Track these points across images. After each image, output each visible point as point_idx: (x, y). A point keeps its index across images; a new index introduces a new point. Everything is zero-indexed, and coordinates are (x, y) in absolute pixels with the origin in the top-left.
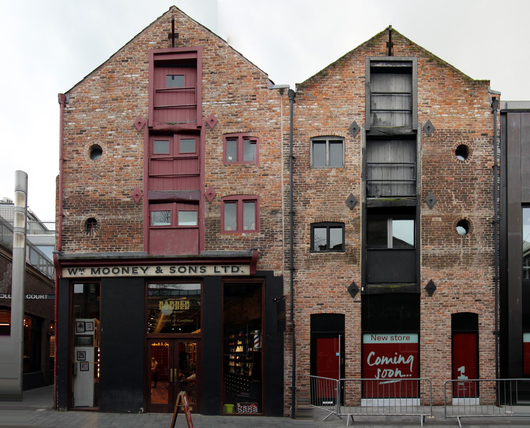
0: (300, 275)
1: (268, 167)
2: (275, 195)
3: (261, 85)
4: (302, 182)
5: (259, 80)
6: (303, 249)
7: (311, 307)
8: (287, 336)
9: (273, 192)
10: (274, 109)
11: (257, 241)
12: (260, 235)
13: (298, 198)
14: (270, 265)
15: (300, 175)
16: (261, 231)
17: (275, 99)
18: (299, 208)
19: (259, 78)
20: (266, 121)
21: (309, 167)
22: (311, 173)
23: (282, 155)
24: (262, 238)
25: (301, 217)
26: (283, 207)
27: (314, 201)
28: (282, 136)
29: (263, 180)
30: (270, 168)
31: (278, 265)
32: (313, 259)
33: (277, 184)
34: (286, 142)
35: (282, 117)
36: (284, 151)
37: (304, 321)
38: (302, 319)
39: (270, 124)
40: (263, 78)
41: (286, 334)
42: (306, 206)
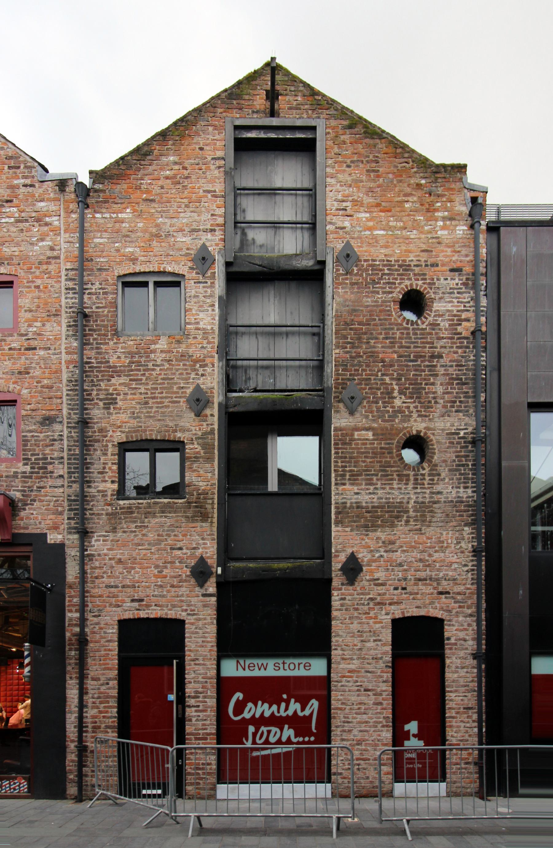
0: (98, 544)
1: (35, 333)
2: (50, 387)
3: (22, 181)
4: (101, 363)
5: (18, 171)
6: (103, 493)
7: (119, 606)
8: (73, 653)
9: (45, 382)
10: (47, 219)
11: (17, 477)
12: (21, 468)
13: (95, 393)
14: (40, 523)
15: (97, 348)
16: (24, 459)
17: (49, 200)
18: (96, 413)
19: (19, 167)
20: (32, 244)
21: (116, 334)
22: (120, 346)
23: (63, 310)
24: (25, 472)
25: (101, 430)
26: (65, 412)
27: (126, 399)
28: (63, 273)
29: (27, 359)
30: (39, 334)
31: (54, 523)
32: (123, 513)
33: (53, 367)
34: (71, 284)
35: (64, 236)
36: (67, 301)
37: (105, 633)
38: (101, 628)
39: (39, 249)
40: (26, 167)
41: (70, 650)
42: (109, 408)
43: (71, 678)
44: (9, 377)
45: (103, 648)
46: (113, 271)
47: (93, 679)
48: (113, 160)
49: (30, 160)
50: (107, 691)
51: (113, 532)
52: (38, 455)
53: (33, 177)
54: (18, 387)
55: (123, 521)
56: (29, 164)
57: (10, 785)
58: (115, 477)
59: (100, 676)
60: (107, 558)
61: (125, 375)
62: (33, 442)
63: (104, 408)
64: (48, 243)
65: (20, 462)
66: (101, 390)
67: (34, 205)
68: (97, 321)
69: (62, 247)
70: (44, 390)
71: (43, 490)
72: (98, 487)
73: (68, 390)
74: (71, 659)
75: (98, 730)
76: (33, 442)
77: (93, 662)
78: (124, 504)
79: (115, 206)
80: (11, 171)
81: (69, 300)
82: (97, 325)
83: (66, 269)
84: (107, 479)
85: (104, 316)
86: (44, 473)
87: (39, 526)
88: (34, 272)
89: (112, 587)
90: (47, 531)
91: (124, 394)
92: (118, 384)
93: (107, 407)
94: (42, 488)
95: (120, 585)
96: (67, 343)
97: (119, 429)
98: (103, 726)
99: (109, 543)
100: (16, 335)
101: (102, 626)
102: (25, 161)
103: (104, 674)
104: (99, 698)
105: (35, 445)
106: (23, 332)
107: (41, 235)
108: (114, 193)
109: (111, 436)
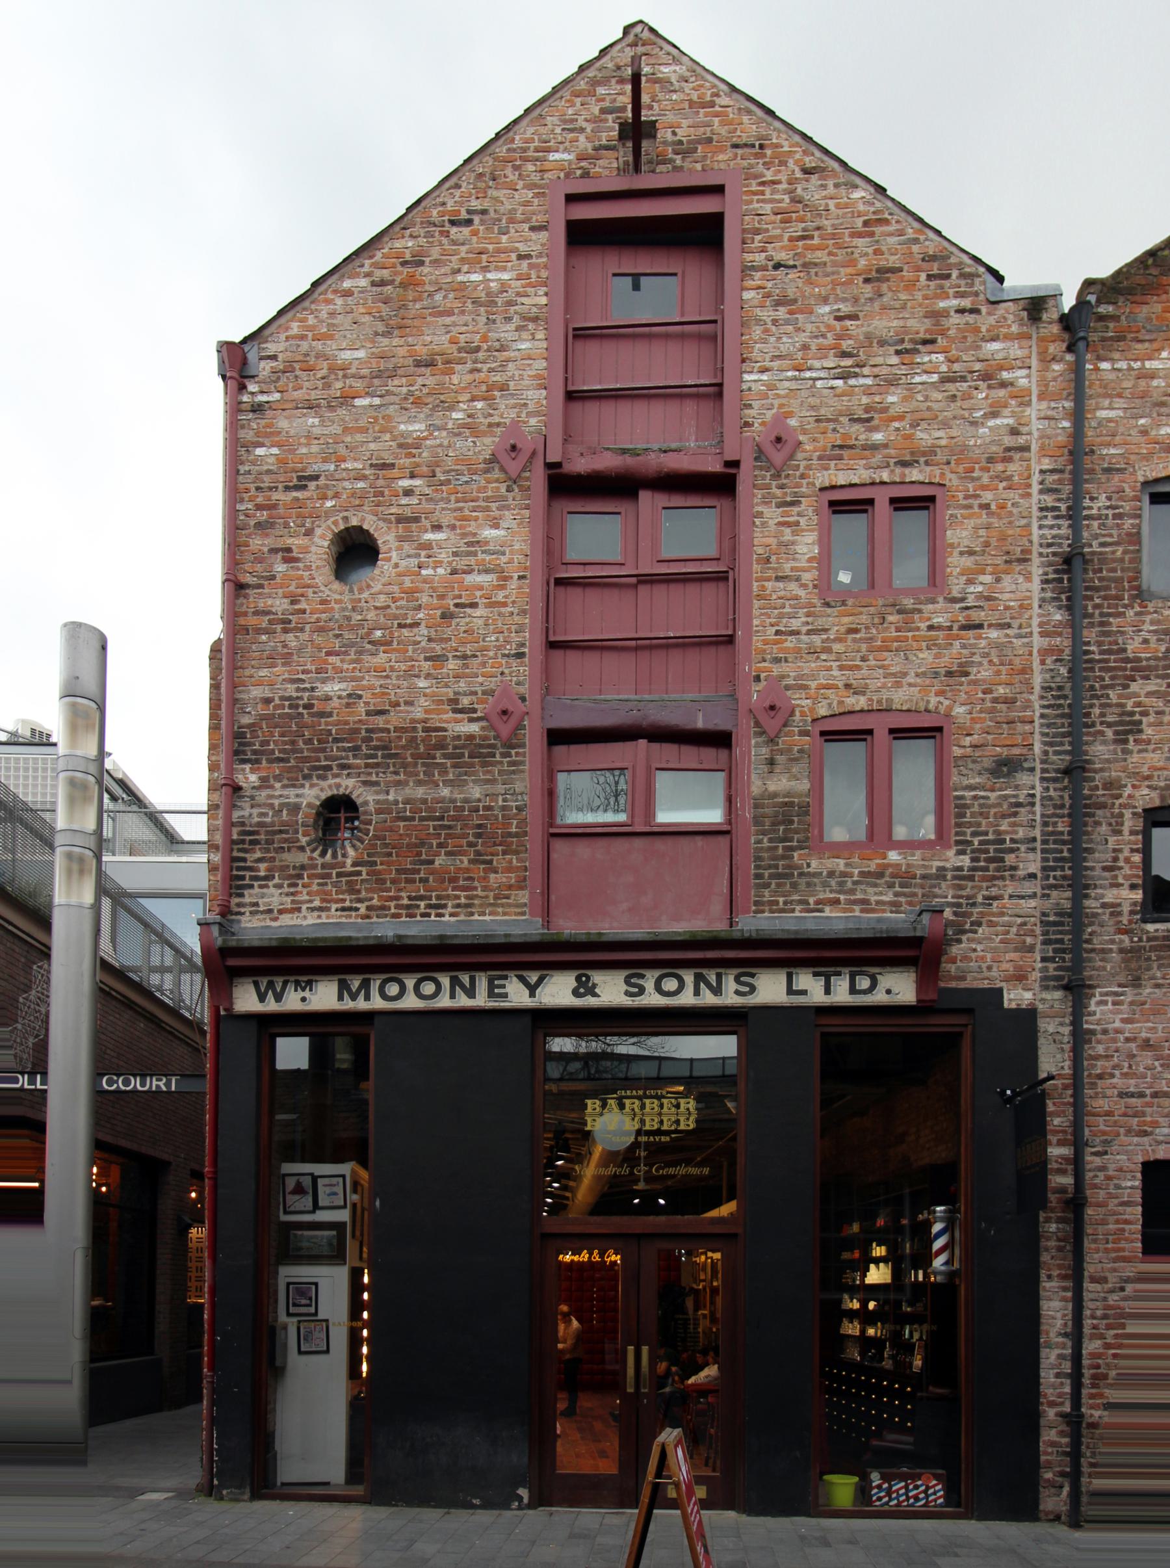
0: (1102, 1011)
1: (980, 596)
2: (1009, 701)
3: (955, 302)
4: (1110, 652)
5: (947, 283)
6: (1114, 909)
7: (1145, 1134)
8: (1053, 1227)
9: (1001, 690)
10: (1005, 375)
11: (944, 878)
12: (953, 859)
13: (1097, 711)
14: (989, 968)
15: (1102, 624)
16: (958, 843)
17: (1008, 337)
18: (1100, 751)
19: (948, 276)
20: (974, 423)
21: (1141, 595)
22: (1148, 618)
23: (1036, 549)
24: (960, 869)
25: (1109, 785)
26: (1038, 748)
27: (1161, 724)
28: (1036, 478)
29: (964, 647)
30: (989, 599)
31: (1018, 968)
32: (1152, 949)
33: (1017, 661)
34: (1049, 500)
35: (1034, 411)
36: (1043, 535)
37: (1118, 1187)
38: (1109, 1178)
39: (990, 432)
40: (962, 276)
41: (1048, 1220)
42: (1126, 741)
43: (1049, 1277)
44: (928, 682)
45: (1111, 1219)
46: (1134, 473)
47: (1094, 1280)
48: (1129, 259)
49: (970, 262)
50: (1121, 1303)
51: (1134, 986)
52: (986, 834)
53: (976, 294)
54: (947, 703)
55: (1155, 965)
56: (967, 270)
57: (907, 1491)
58: (1137, 876)
59: (1107, 1274)
60: (1121, 1037)
61: (1157, 677)
62: (976, 809)
63: (1116, 741)
64: (1006, 421)
65: (950, 847)
66: (1109, 705)
67: (979, 348)
68: (1101, 570)
69: (1034, 428)
70: (999, 706)
71: (995, 904)
72: (1103, 896)
73: (1044, 707)
74: (1048, 1239)
75: (1101, 1383)
76: (976, 809)
77: (1093, 1246)
78: (1157, 931)
79: (1139, 346)
80: (932, 284)
81: (1046, 531)
82: (1101, 579)
83: (1042, 472)
84: (1121, 880)
85: (1114, 560)
86: (997, 870)
87: (986, 974)
88: (979, 478)
89: (1132, 1095)
90: (1003, 984)
91: (1157, 713)
92: (1143, 693)
93: (1121, 739)
94: (995, 898)
95: (1148, 1092)
96: (1043, 615)
97: (1147, 783)
98: (1113, 1373)
99: (1124, 1007)
100: (941, 599)
101: (1111, 1173)
102: (961, 263)
103: (1115, 1270)
104: (1105, 1317)
105: (981, 814)
106: (955, 594)
107: (991, 406)
108: (1135, 321)
109: (1130, 796)
